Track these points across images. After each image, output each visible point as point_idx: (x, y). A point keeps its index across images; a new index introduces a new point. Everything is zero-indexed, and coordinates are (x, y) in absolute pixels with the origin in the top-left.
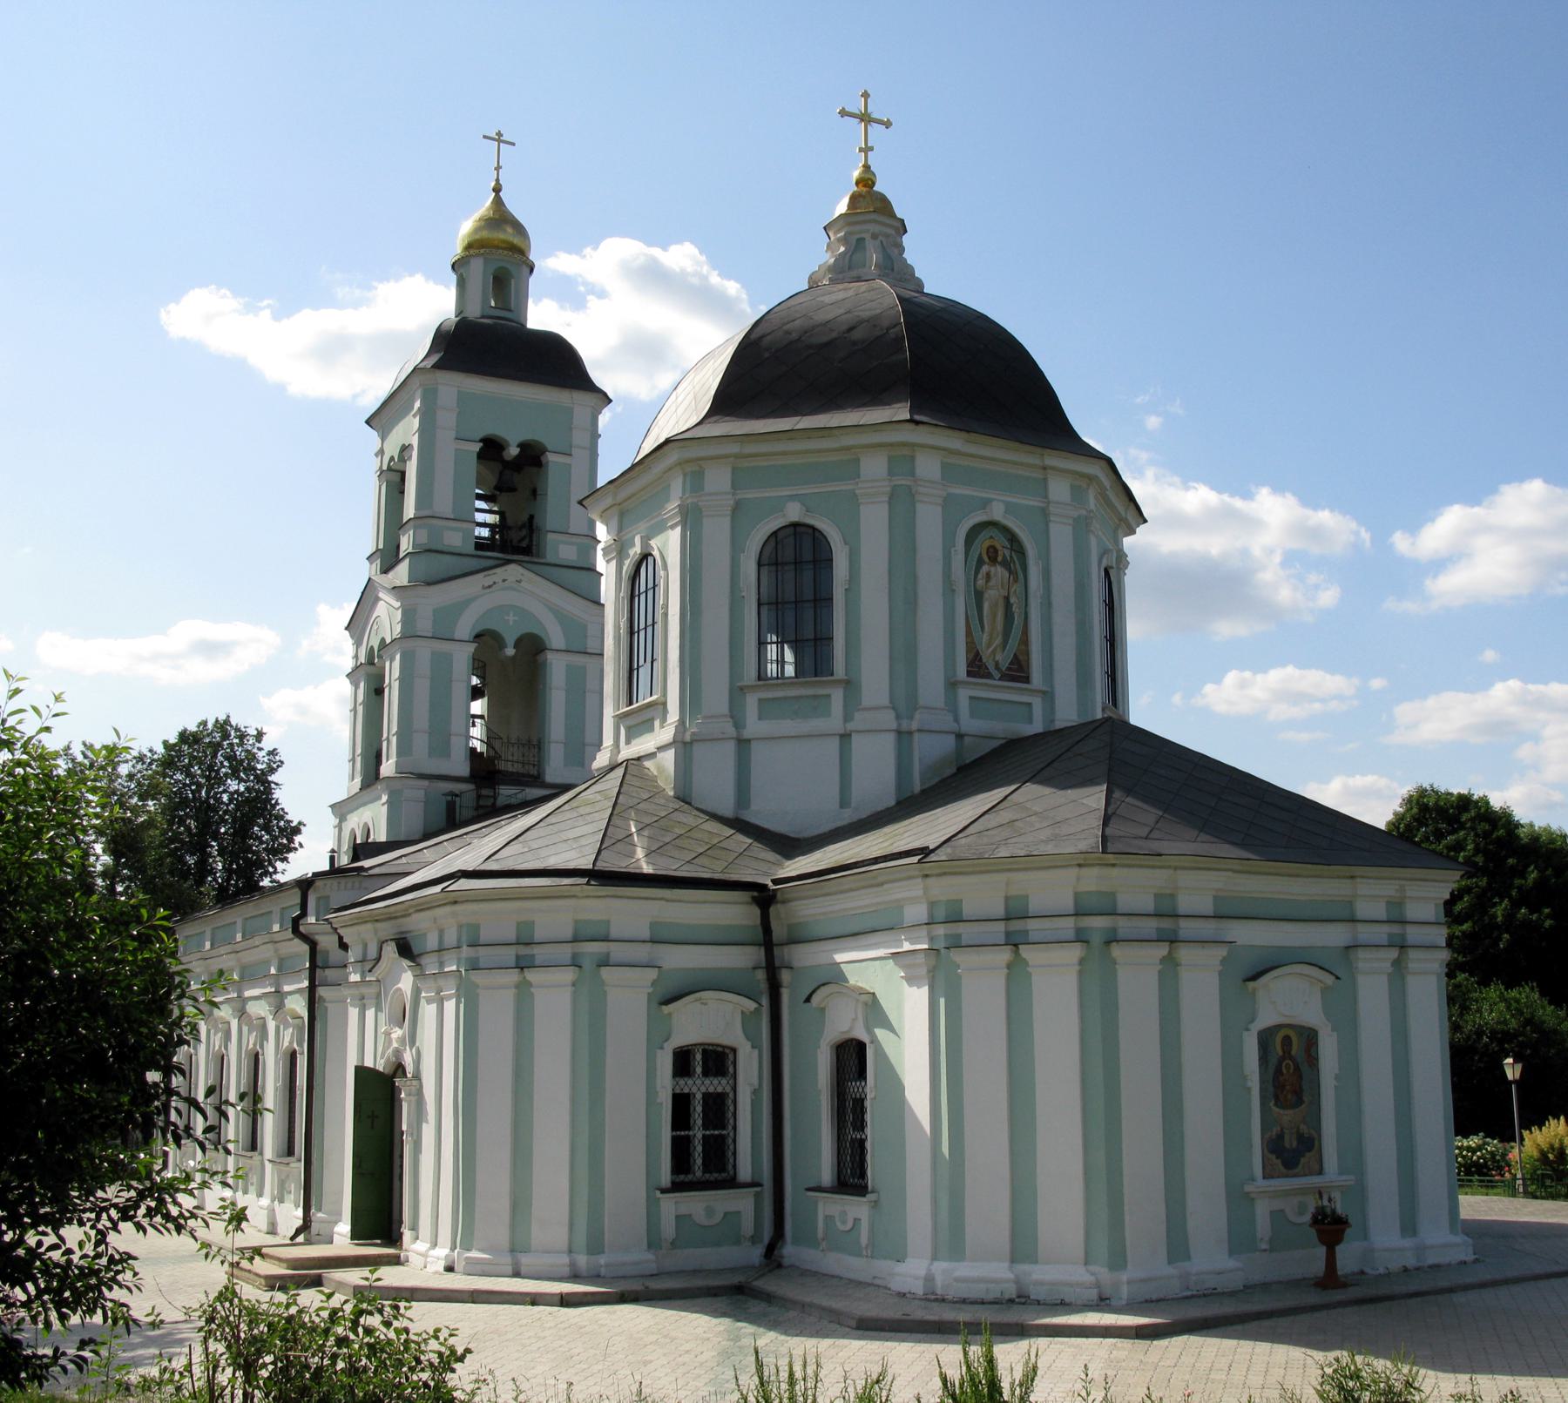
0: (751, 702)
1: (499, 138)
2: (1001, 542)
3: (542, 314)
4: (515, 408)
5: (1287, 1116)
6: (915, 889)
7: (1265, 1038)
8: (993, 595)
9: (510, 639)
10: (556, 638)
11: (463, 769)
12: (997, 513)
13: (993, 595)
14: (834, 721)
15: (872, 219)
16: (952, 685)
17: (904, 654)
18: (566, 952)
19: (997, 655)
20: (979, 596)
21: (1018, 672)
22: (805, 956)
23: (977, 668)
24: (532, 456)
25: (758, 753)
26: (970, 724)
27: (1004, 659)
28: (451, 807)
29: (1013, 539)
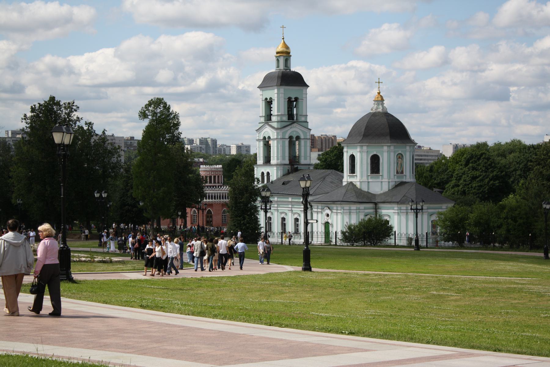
0: (369, 177)
1: (283, 27)
2: (400, 156)
3: (295, 68)
4: (293, 91)
5: (434, 230)
6: (396, 206)
7: (432, 222)
8: (399, 163)
9: (295, 137)
10: (302, 137)
11: (287, 162)
12: (400, 152)
13: (399, 163)
14: (380, 180)
15: (380, 100)
16: (395, 175)
17: (389, 172)
18: (355, 211)
19: (400, 171)
20: (398, 163)
21: (402, 172)
22: (379, 211)
23: (397, 173)
24: (296, 99)
25: (370, 184)
26: (397, 180)
27: (400, 171)
28: (288, 170)
29: (402, 155)
